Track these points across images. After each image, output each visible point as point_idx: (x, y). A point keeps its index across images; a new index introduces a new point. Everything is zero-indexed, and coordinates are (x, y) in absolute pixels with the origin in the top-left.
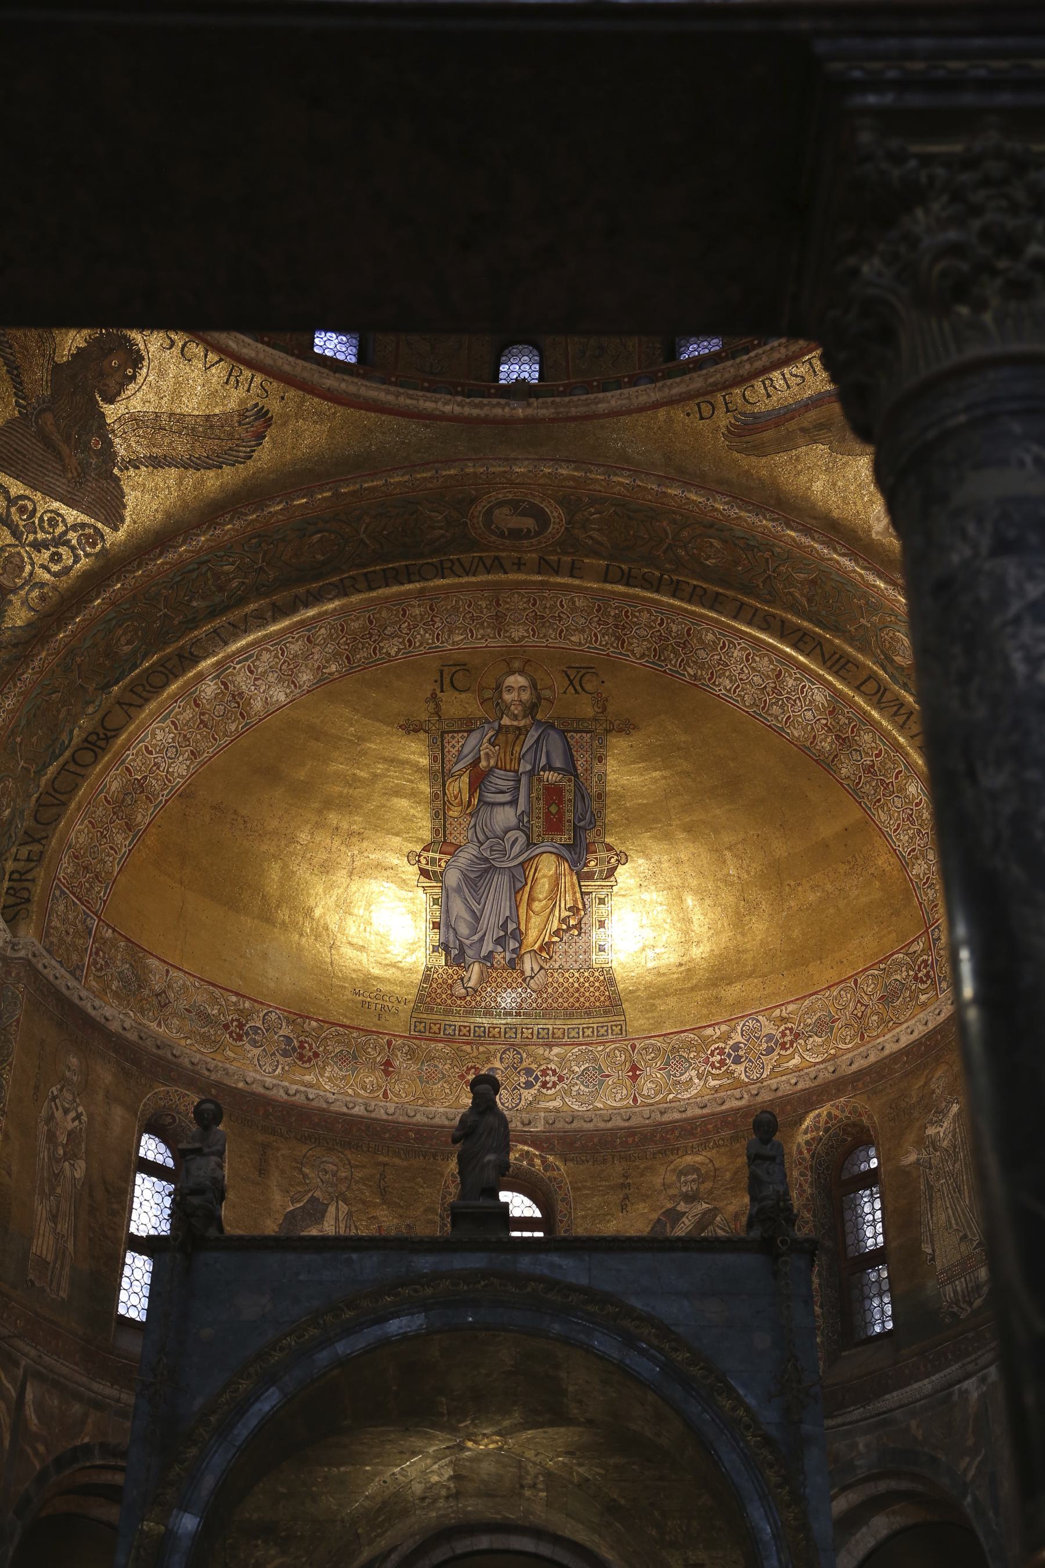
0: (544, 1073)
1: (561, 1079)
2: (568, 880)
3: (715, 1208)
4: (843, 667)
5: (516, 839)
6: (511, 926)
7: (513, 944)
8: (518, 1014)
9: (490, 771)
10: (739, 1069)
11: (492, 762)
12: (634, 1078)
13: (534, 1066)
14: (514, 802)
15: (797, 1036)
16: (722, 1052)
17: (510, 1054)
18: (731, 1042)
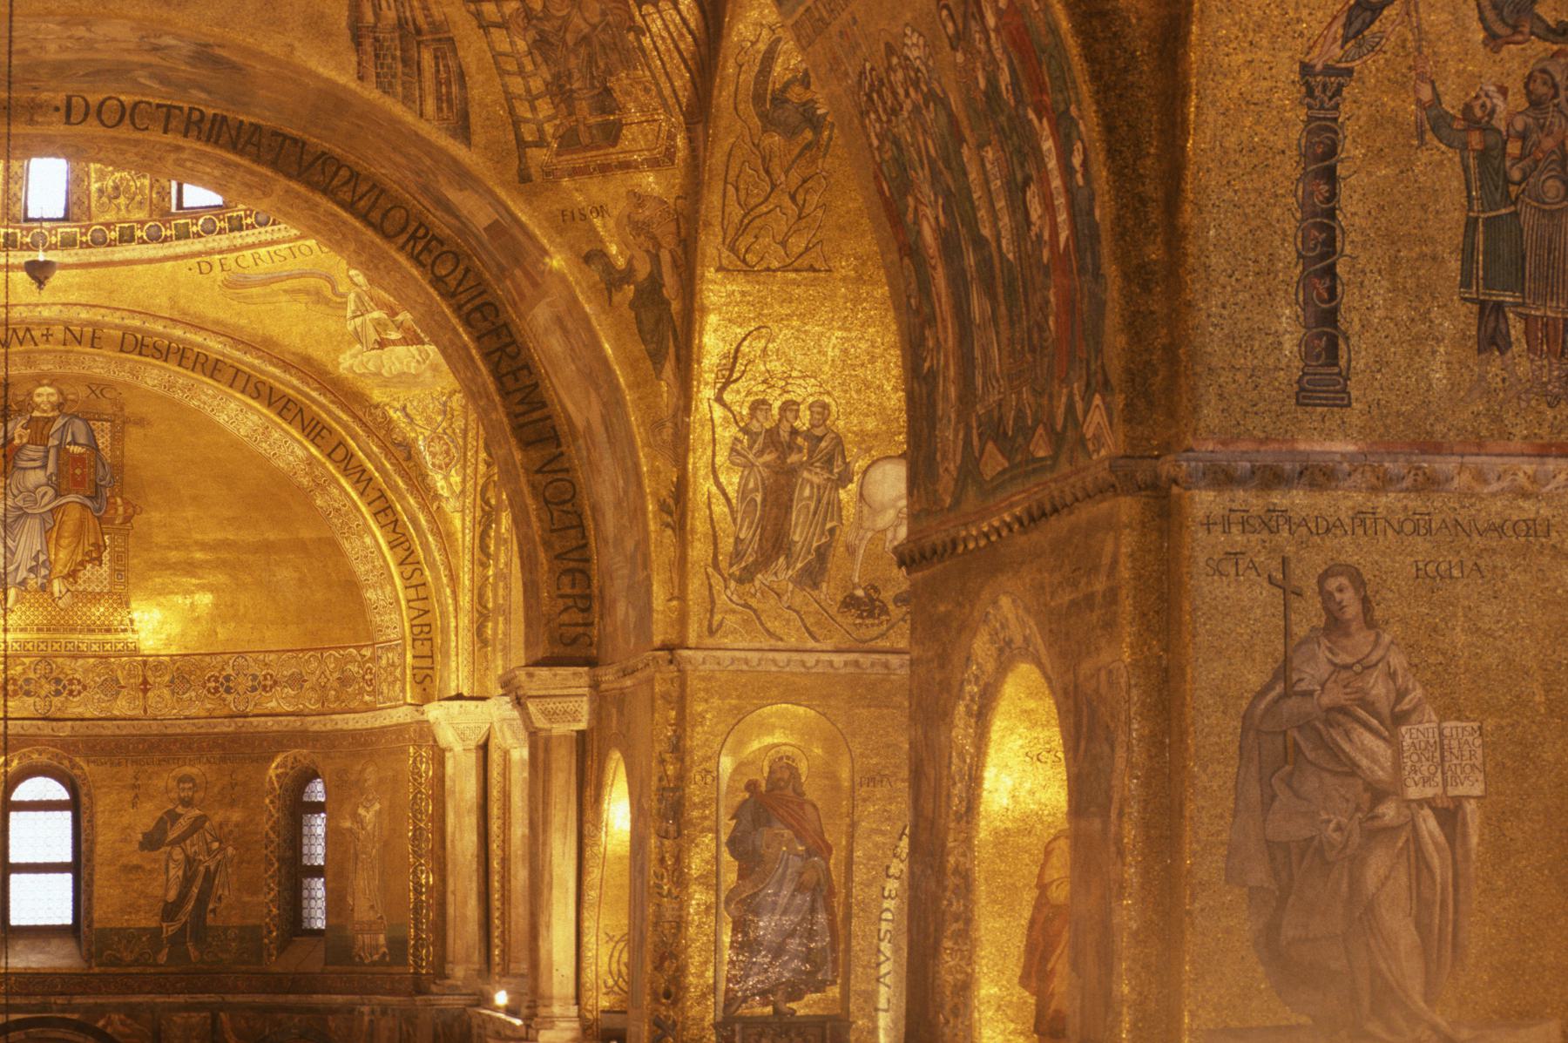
0: (71, 682)
1: (85, 687)
2: (92, 523)
3: (205, 816)
4: (319, 434)
5: (45, 493)
6: (42, 558)
7: (44, 572)
8: (49, 630)
9: (21, 447)
10: (230, 698)
11: (25, 440)
12: (145, 691)
13: (61, 676)
14: (44, 467)
15: (276, 683)
16: (216, 681)
17: (43, 665)
18: (224, 673)
